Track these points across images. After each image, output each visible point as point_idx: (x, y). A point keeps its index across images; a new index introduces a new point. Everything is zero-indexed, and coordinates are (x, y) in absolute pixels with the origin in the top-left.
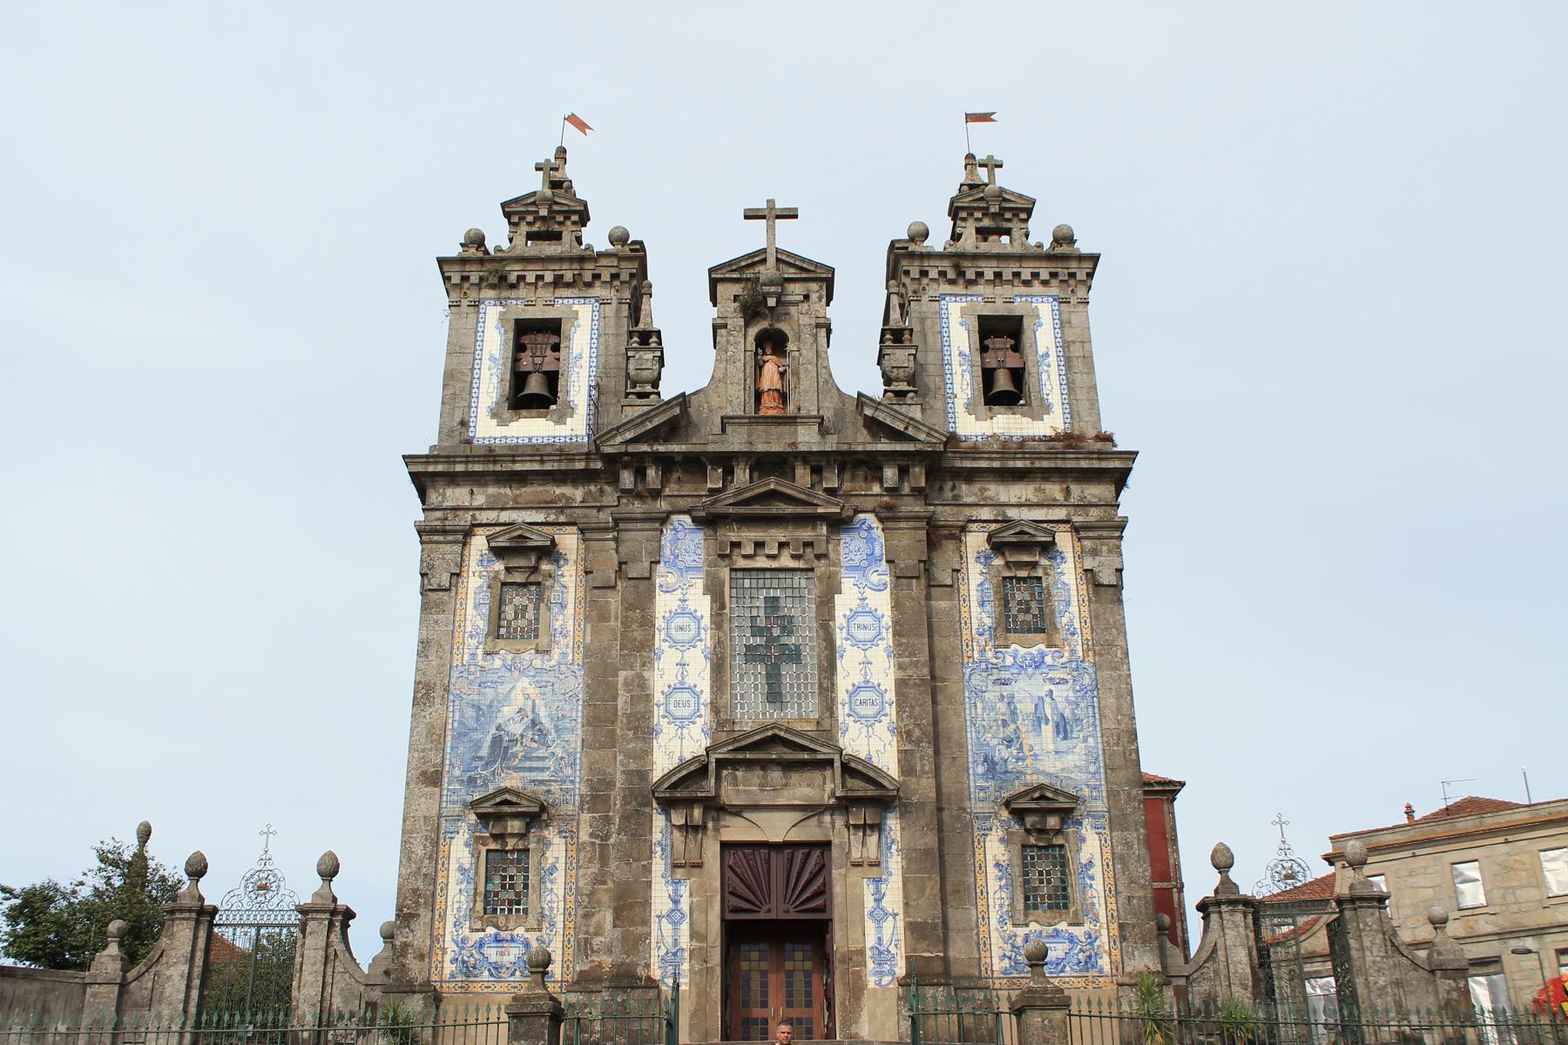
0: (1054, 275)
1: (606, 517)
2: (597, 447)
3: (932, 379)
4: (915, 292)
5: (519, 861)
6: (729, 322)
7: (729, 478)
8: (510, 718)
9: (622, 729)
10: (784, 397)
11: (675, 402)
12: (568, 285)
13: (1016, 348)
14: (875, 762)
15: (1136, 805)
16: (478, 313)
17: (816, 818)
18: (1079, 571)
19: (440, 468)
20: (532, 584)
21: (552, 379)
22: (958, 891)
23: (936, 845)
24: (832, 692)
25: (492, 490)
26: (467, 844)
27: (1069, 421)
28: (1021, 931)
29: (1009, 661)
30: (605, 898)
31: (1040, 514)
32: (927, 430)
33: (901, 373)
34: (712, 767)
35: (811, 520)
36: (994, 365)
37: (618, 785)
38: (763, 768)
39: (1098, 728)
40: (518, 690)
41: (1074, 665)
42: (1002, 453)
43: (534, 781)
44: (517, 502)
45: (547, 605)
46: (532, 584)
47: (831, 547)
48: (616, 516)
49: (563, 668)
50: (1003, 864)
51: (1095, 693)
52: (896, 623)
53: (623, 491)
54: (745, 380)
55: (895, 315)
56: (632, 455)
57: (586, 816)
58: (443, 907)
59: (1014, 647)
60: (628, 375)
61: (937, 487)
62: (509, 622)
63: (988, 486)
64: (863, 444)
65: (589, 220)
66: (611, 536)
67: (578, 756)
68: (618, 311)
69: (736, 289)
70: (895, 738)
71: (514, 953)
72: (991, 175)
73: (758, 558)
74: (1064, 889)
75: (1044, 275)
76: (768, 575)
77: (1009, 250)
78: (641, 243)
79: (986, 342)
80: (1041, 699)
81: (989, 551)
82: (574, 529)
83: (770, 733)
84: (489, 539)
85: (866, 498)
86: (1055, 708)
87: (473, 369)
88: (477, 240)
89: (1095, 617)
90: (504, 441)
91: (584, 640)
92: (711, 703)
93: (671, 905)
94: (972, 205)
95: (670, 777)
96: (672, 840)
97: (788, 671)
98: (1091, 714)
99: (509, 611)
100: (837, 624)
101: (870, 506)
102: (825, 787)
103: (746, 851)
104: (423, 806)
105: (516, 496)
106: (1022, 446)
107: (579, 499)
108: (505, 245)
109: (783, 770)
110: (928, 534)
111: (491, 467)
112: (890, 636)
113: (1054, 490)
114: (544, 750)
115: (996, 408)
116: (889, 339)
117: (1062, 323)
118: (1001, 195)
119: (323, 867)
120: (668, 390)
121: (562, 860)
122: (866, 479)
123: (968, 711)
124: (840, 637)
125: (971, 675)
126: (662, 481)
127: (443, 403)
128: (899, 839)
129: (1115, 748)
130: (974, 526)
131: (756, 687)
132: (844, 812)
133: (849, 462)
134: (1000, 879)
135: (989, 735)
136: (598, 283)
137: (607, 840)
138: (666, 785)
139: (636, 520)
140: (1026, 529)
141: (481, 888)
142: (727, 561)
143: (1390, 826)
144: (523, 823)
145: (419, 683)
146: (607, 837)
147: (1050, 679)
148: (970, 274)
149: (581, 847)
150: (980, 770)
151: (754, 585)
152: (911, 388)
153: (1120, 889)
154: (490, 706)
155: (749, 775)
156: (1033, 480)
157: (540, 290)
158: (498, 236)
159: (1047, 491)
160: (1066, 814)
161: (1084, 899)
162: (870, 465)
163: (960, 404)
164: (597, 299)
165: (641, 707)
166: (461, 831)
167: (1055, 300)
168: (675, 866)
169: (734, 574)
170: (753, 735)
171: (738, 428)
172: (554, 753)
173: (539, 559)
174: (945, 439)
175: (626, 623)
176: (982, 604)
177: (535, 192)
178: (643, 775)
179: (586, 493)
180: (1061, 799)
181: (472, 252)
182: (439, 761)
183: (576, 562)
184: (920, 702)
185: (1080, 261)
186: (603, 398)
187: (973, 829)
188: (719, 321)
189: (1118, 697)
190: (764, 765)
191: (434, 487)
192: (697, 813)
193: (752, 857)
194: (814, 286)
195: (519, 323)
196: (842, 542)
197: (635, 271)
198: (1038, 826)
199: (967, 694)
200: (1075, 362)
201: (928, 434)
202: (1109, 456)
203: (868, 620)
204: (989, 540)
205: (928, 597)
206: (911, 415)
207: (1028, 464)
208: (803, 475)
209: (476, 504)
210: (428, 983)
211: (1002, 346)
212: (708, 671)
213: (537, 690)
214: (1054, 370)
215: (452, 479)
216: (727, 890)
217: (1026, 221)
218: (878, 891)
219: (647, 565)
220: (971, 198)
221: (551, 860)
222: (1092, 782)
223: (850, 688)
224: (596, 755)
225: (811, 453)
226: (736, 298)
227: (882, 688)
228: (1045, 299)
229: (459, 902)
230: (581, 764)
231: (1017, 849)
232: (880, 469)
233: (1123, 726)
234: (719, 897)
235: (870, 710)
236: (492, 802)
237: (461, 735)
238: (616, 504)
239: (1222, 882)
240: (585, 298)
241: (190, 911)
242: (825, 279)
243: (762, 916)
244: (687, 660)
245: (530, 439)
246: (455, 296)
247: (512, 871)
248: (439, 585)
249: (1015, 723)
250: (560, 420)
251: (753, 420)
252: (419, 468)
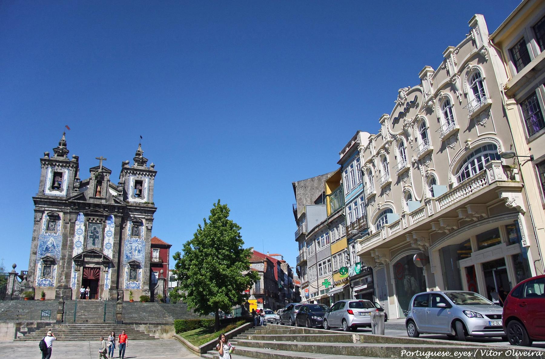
0: (149, 174)
10: (100, 192)
13: (141, 186)
25: (48, 204)
28: (129, 282)
29: (132, 240)
40: (51, 239)
57: (61, 261)
68: (73, 172)
69: (94, 173)
71: (48, 282)
84: (47, 213)
89: (147, 234)
97: (96, 240)
99: (50, 225)
102: (101, 260)
111: (48, 200)
122: (113, 209)
124: (105, 235)
141: (43, 272)
146: (64, 264)
148: (135, 172)
149: (60, 266)
150: (125, 257)
165: (72, 244)
168: (76, 270)
176: (129, 231)
178: (71, 255)
189: (148, 247)
203: (110, 232)
210: (33, 286)
214: (146, 191)
226: (94, 174)
237: (41, 246)
243: (89, 278)
246: (43, 166)
252: (35, 199)
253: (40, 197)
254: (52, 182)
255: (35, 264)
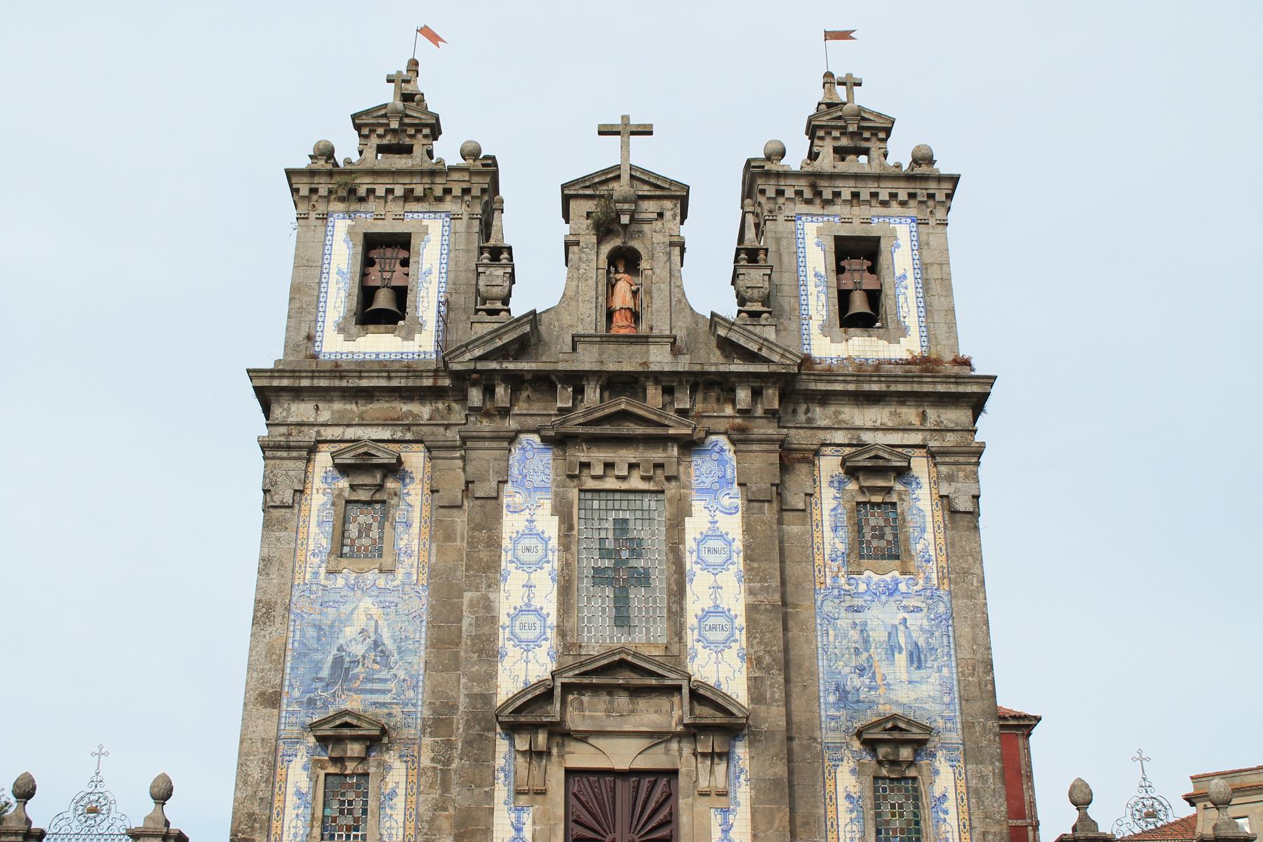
0: (912, 196)
1: (453, 435)
2: (446, 364)
3: (787, 300)
4: (770, 211)
5: (358, 786)
6: (582, 239)
7: (580, 397)
8: (352, 639)
9: (466, 652)
10: (636, 316)
11: (525, 319)
12: (418, 199)
13: (873, 270)
14: (724, 688)
15: (992, 737)
16: (327, 226)
17: (663, 746)
18: (935, 496)
19: (285, 383)
20: (377, 502)
21: (401, 294)
22: (808, 823)
23: (786, 775)
24: (681, 616)
25: (338, 406)
26: (305, 768)
27: (926, 344)
29: (862, 588)
30: (445, 825)
31: (895, 439)
32: (781, 352)
33: (756, 293)
34: (558, 691)
35: (662, 441)
36: (850, 287)
37: (461, 708)
38: (610, 693)
39: (953, 658)
40: (361, 611)
41: (928, 593)
42: (857, 376)
43: (375, 703)
44: (363, 419)
45: (391, 524)
46: (377, 502)
47: (682, 469)
48: (463, 434)
49: (407, 588)
50: (855, 796)
51: (950, 622)
52: (747, 547)
53: (471, 409)
54: (597, 298)
55: (750, 234)
56: (481, 372)
57: (427, 740)
58: (279, 832)
59: (867, 573)
60: (478, 291)
61: (790, 410)
62: (353, 541)
63: (842, 410)
64: (716, 364)
65: (440, 133)
66: (458, 455)
67: (421, 678)
68: (469, 226)
69: (590, 206)
70: (745, 665)
72: (850, 94)
73: (607, 479)
74: (917, 823)
75: (903, 196)
76: (617, 496)
77: (867, 170)
78: (493, 158)
79: (842, 263)
80: (895, 627)
81: (843, 476)
82: (421, 446)
83: (617, 658)
85: (718, 420)
86: (909, 636)
87: (320, 283)
88: (326, 153)
89: (951, 544)
90: (350, 356)
91: (429, 560)
92: (558, 626)
93: (513, 833)
94: (830, 123)
95: (513, 702)
96: (515, 766)
97: (637, 595)
98: (945, 643)
99: (353, 530)
100: (687, 547)
101: (722, 429)
103: (591, 778)
104: (261, 728)
105: (362, 412)
106: (878, 369)
107: (426, 416)
108: (355, 158)
109: (631, 696)
110: (781, 457)
111: (337, 383)
112: (741, 560)
113: (910, 414)
114: (384, 673)
115: (852, 330)
116: (744, 259)
117: (920, 245)
118: (860, 114)
119: (156, 790)
120: (518, 308)
121: (402, 785)
122: (718, 400)
123: (819, 639)
124: (689, 561)
125: (823, 601)
126: (511, 399)
127: (289, 317)
128: (748, 768)
129: (970, 679)
130: (828, 450)
131: (604, 610)
132: (693, 739)
133: (703, 383)
134: (851, 811)
135: (841, 663)
136: (448, 198)
137: (448, 765)
138: (510, 710)
139: (483, 438)
140: (881, 454)
141: (319, 814)
142: (576, 482)
143: (1255, 766)
144: (364, 746)
145: (260, 601)
146: (448, 762)
147: (905, 607)
148: (827, 194)
149: (422, 772)
150: (832, 698)
151: (603, 507)
152: (765, 309)
153: (975, 824)
154: (332, 626)
155: (595, 700)
156: (889, 404)
157: (389, 203)
158: (348, 148)
159: (903, 415)
160: (919, 744)
161: (938, 834)
162: (722, 385)
163: (814, 326)
164: (448, 213)
165: (486, 630)
166: (299, 755)
167: (913, 221)
168: (519, 793)
169: (582, 495)
170: (599, 660)
171: (588, 347)
172: (396, 676)
173: (384, 477)
174: (799, 361)
175: (472, 544)
176: (835, 529)
177: (386, 105)
178: (487, 699)
179: (433, 411)
180: (914, 730)
181: (321, 164)
182: (278, 681)
183: (422, 480)
184: (771, 628)
185: (939, 182)
186: (452, 315)
187: (823, 760)
188: (572, 238)
190: (611, 690)
191: (278, 402)
192: (542, 738)
193: (597, 785)
194: (668, 204)
195: (367, 237)
196: (693, 464)
197: (486, 186)
198: (891, 758)
199: (818, 621)
200: (933, 285)
201: (782, 356)
202: (967, 380)
204: (843, 464)
205: (780, 522)
206: (765, 336)
207: (883, 387)
208: (654, 395)
209: (321, 419)
211: (858, 267)
212: (555, 593)
213: (381, 611)
214: (911, 293)
215: (297, 393)
216: (571, 820)
217: (885, 140)
218: (725, 821)
219: (494, 484)
220: (829, 117)
221: (391, 785)
222: (946, 713)
223: (700, 613)
224: (439, 677)
225: (662, 373)
226: (589, 215)
227: (732, 613)
228: (903, 220)
229: (296, 827)
230: (423, 687)
231: (868, 780)
232: (733, 390)
233: (979, 656)
234: (562, 826)
235: (719, 636)
236: (332, 725)
238: (464, 422)
239: (1080, 819)
240: (435, 212)
241: (16, 834)
242: (680, 197)
244: (533, 582)
245: (377, 355)
246: (303, 208)
247: (351, 796)
248: (282, 502)
249: (868, 651)
250: (408, 336)
251: (604, 339)
252: (264, 383)
253: (290, 368)
254: (356, 291)
255: (273, 767)
